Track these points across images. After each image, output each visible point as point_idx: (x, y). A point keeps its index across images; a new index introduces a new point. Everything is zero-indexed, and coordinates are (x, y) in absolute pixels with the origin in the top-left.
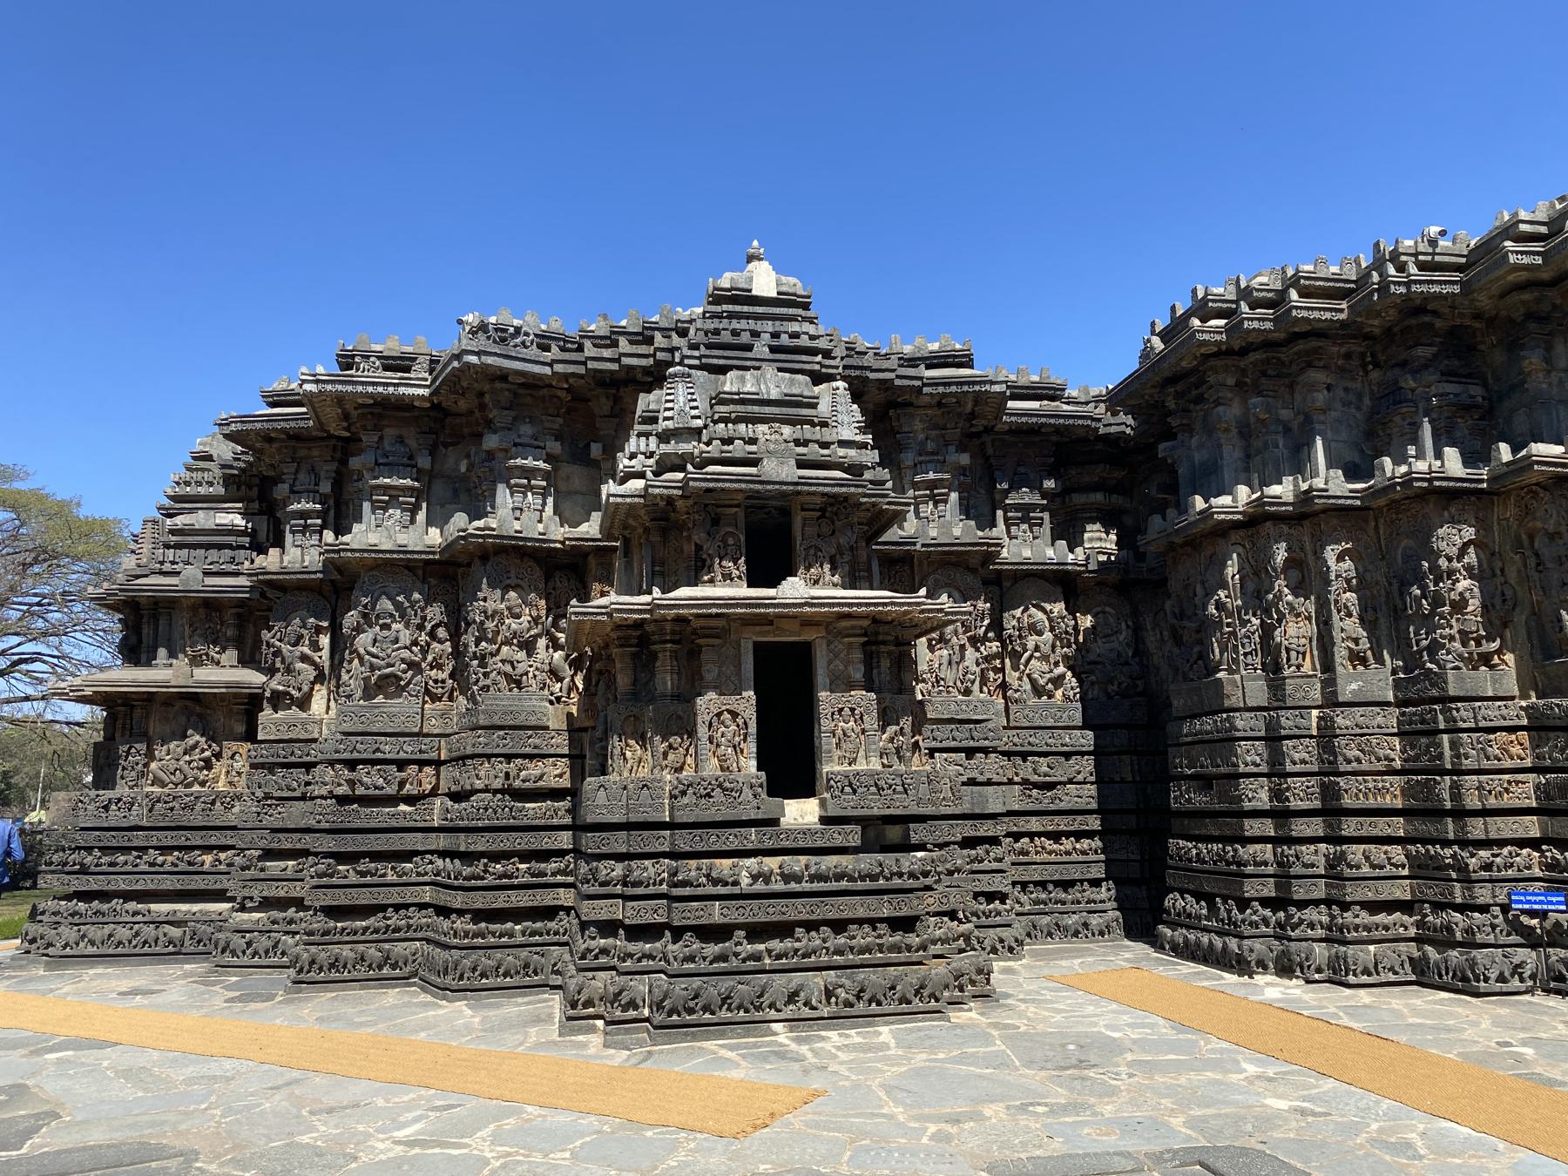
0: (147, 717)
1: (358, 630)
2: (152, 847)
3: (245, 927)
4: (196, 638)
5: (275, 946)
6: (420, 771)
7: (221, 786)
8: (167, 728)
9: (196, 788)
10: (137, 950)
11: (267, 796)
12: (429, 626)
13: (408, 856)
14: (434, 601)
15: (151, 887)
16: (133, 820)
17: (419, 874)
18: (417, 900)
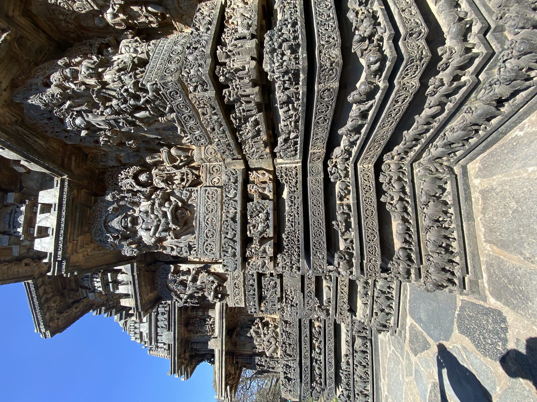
0: (242, 355)
1: (140, 242)
2: (311, 355)
3: (368, 312)
4: (203, 330)
5: (384, 293)
6: (253, 182)
7: (277, 316)
8: (248, 345)
9: (278, 330)
10: (370, 363)
11: (280, 300)
12: (137, 188)
13: (328, 186)
14: (117, 185)
15: (333, 355)
16: (295, 365)
17: (347, 176)
18: (372, 176)
